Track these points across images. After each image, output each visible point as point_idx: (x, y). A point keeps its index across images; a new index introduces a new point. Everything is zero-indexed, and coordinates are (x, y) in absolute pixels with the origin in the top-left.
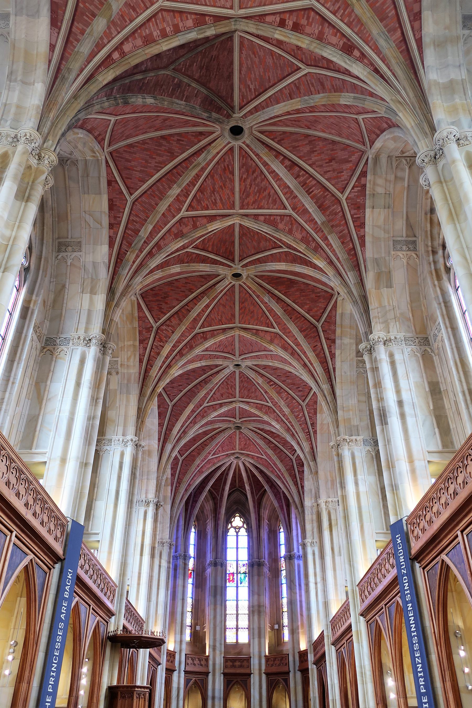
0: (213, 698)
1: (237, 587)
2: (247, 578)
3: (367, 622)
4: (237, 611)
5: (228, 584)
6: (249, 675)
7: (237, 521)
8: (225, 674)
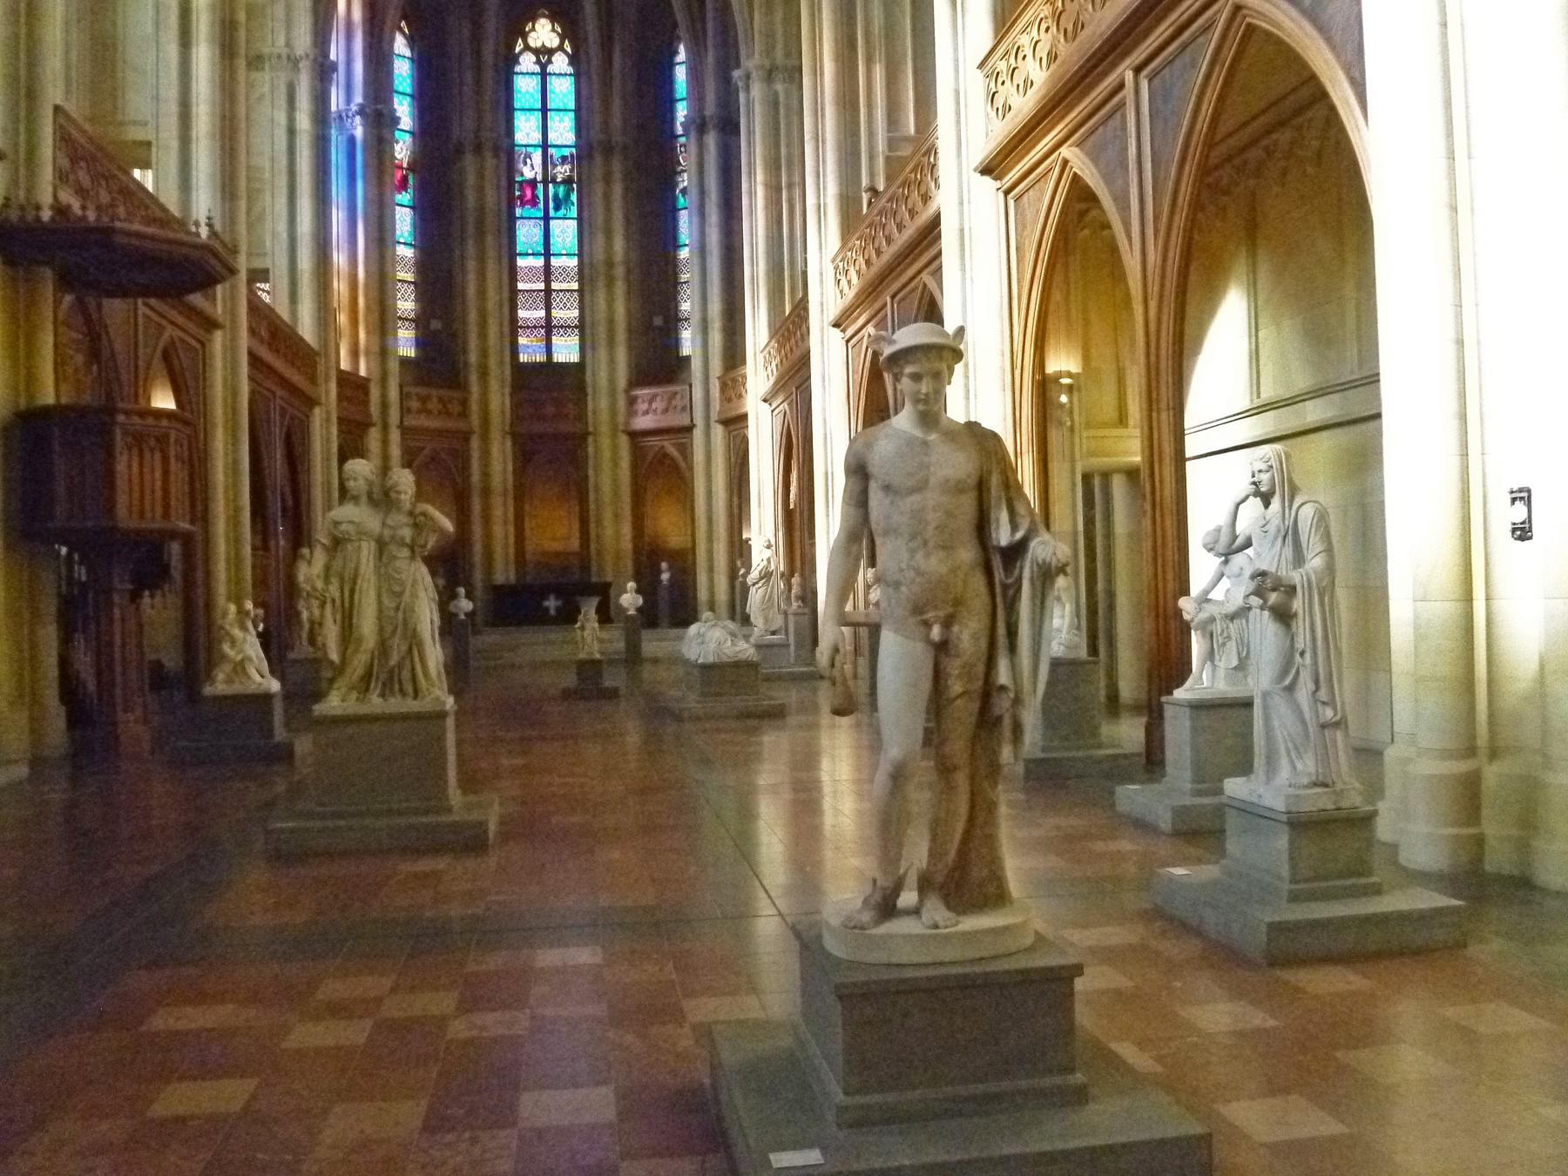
0: (486, 492)
1: (546, 218)
2: (574, 197)
3: (1007, 193)
4: (548, 282)
5: (518, 212)
6: (584, 436)
7: (543, 33)
8: (515, 436)
